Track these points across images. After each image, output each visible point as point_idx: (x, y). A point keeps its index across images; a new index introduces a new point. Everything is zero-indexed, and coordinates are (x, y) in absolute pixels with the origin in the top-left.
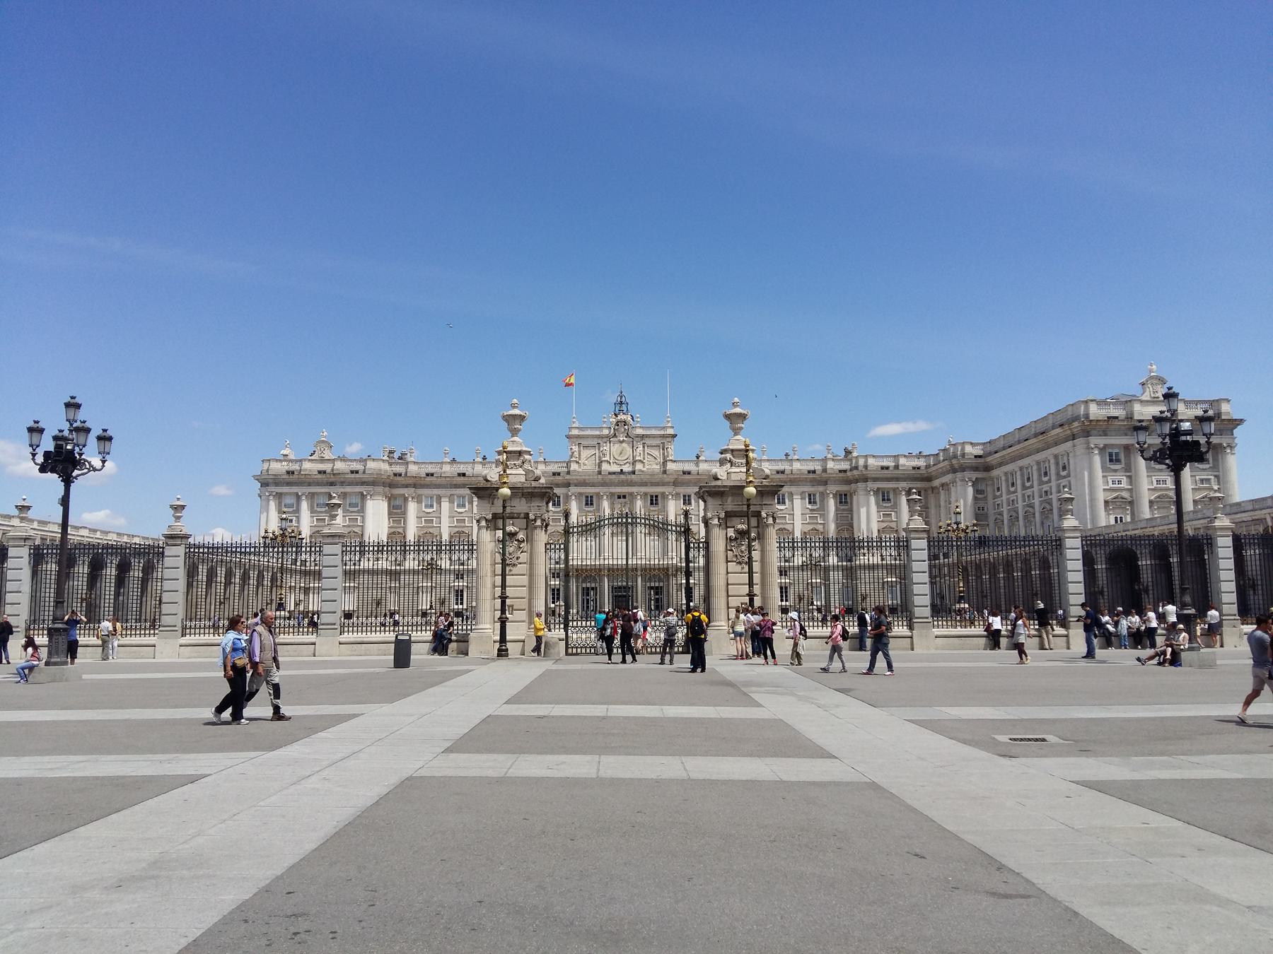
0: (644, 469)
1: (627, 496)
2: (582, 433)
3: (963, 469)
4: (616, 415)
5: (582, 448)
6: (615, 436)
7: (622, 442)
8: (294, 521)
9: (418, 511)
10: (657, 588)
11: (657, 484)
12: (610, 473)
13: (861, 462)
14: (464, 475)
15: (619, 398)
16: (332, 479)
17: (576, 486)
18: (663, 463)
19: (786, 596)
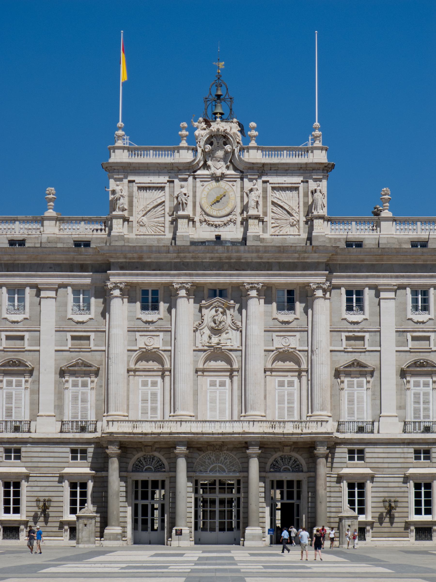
0: (266, 236)
1: (230, 291)
4: (208, 123)
5: (135, 189)
6: (206, 166)
10: (290, 483)
12: (193, 243)
15: (214, 88)
17: (122, 268)
18: (306, 223)
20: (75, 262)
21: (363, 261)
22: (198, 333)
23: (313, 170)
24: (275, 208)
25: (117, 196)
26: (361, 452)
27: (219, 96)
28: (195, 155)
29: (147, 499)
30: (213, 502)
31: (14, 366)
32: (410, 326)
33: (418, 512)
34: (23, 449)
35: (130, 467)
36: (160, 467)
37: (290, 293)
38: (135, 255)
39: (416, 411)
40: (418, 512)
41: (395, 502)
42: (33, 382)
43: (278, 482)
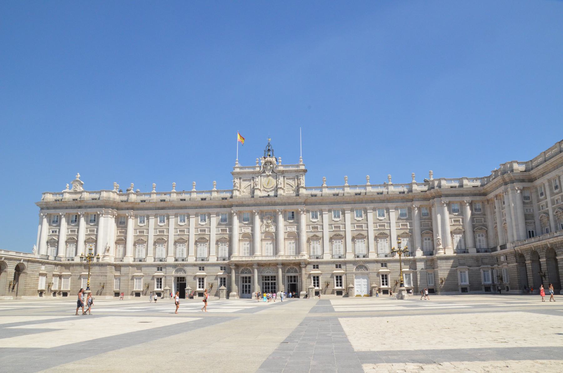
0: (284, 194)
2: (242, 171)
3: (512, 182)
4: (265, 158)
5: (242, 180)
7: (268, 176)
8: (57, 232)
9: (135, 226)
10: (295, 277)
11: (293, 204)
13: (436, 183)
14: (164, 201)
15: (267, 147)
16: (79, 204)
17: (237, 206)
19: (386, 281)
20: (222, 205)
21: (317, 201)
22: (262, 227)
23: (300, 172)
24: (287, 185)
25: (235, 183)
26: (317, 266)
27: (269, 149)
28: (260, 169)
29: (247, 283)
30: (269, 283)
31: (202, 239)
32: (333, 223)
33: (337, 286)
34: (205, 267)
35: (240, 272)
36: (250, 272)
37: (293, 213)
38: (241, 202)
39: (336, 251)
40: (337, 286)
41: (329, 282)
42: (208, 244)
43: (290, 276)
